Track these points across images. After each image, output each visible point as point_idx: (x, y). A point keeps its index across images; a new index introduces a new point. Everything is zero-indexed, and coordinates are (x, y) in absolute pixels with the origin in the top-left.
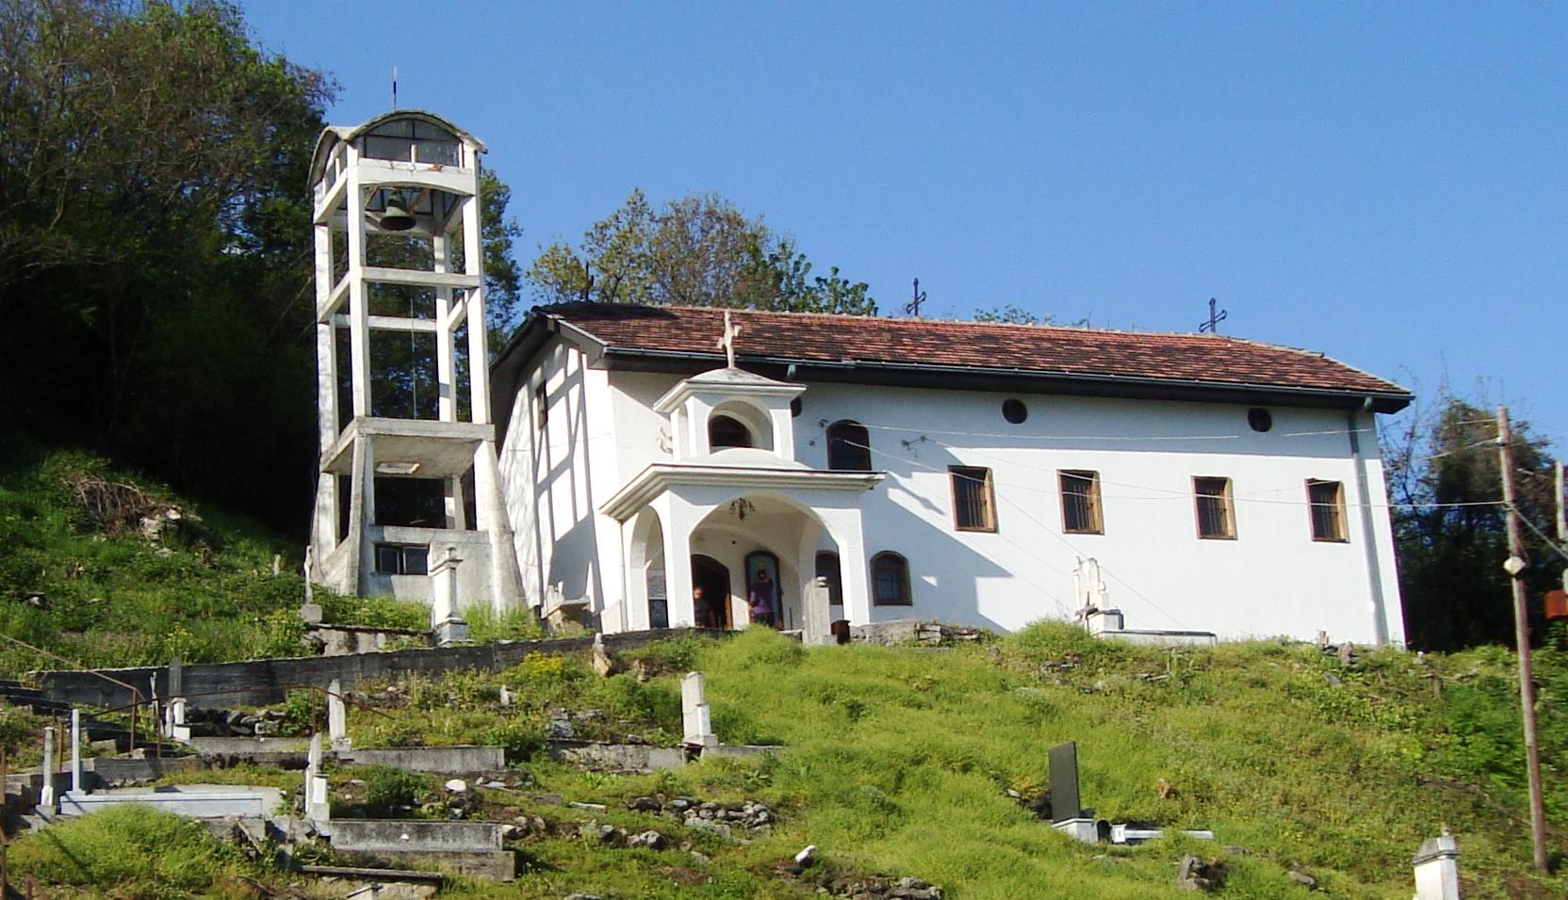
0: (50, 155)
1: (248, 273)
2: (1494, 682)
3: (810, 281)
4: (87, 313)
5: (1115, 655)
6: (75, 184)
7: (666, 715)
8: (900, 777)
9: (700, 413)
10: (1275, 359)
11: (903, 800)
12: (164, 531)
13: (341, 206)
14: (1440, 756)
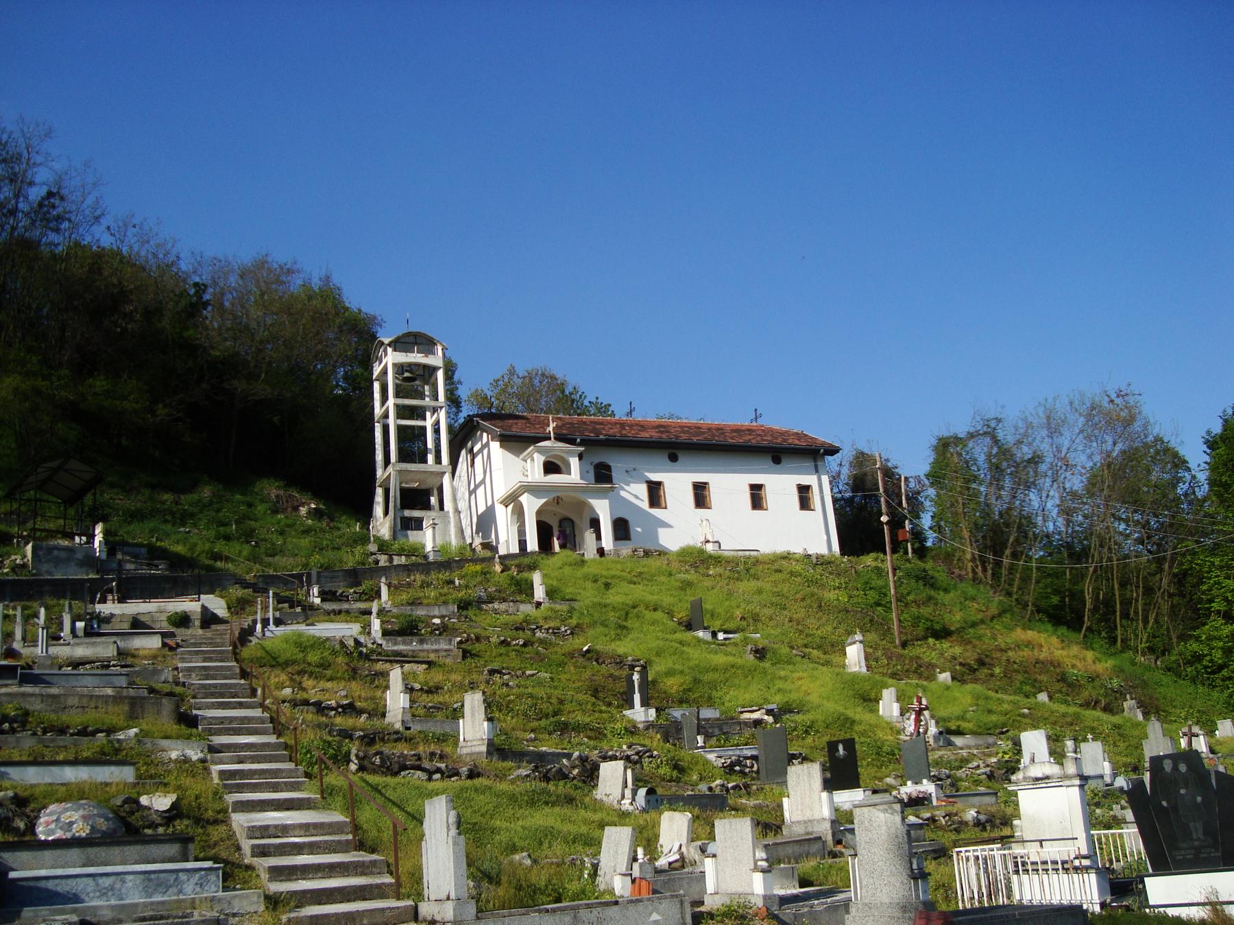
0: (260, 350)
1: (344, 402)
2: (877, 568)
3: (586, 403)
4: (276, 419)
5: (717, 560)
6: (270, 363)
7: (526, 589)
8: (627, 614)
9: (539, 459)
10: (783, 434)
11: (629, 624)
12: (309, 512)
13: (384, 372)
14: (855, 600)
